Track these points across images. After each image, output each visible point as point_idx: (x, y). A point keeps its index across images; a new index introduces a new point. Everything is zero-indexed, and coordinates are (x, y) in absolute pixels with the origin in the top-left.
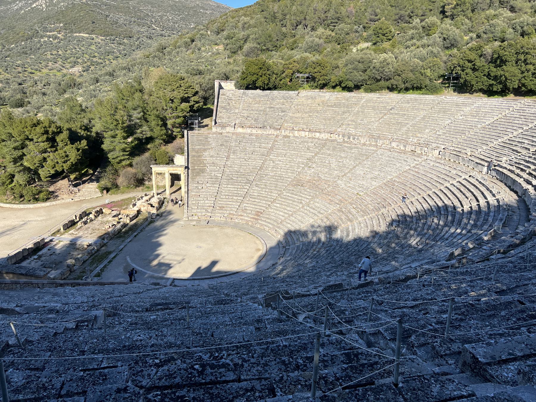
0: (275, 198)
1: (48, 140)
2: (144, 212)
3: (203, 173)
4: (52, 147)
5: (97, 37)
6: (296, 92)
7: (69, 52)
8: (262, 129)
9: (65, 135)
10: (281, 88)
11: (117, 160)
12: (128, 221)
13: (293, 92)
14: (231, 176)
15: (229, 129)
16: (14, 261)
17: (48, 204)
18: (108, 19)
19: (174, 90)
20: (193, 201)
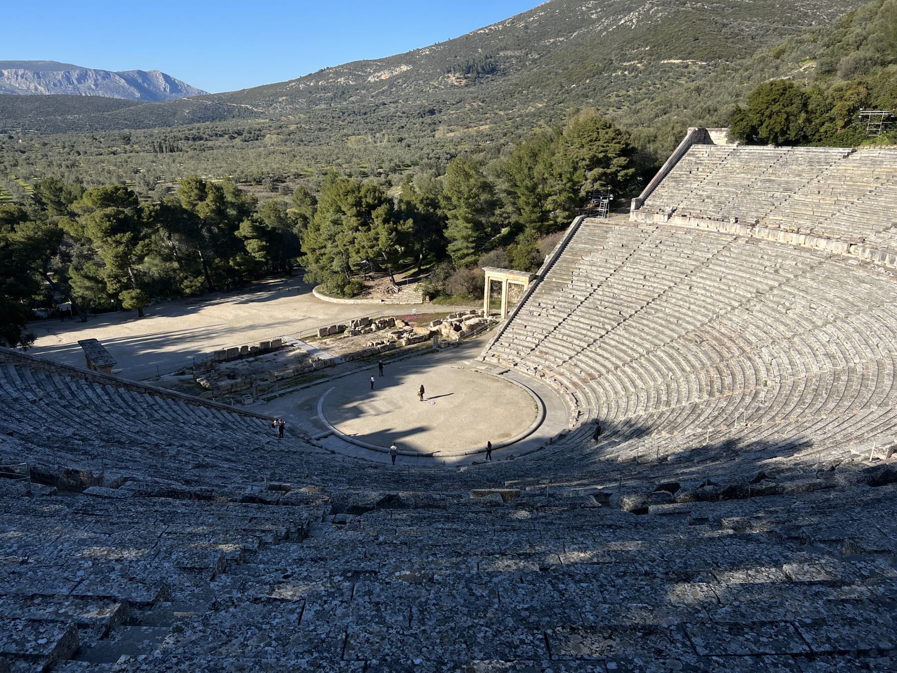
0: (636, 356)
1: (359, 214)
2: (445, 335)
3: (558, 290)
4: (362, 225)
5: (694, 63)
6: (848, 150)
7: (644, 90)
8: (718, 223)
9: (381, 210)
10: (820, 142)
11: (459, 254)
12: (404, 344)
13: (841, 150)
14: (599, 303)
15: (660, 219)
16: (222, 357)
17: (352, 301)
18: (724, 30)
19: (583, 146)
20: (510, 333)
